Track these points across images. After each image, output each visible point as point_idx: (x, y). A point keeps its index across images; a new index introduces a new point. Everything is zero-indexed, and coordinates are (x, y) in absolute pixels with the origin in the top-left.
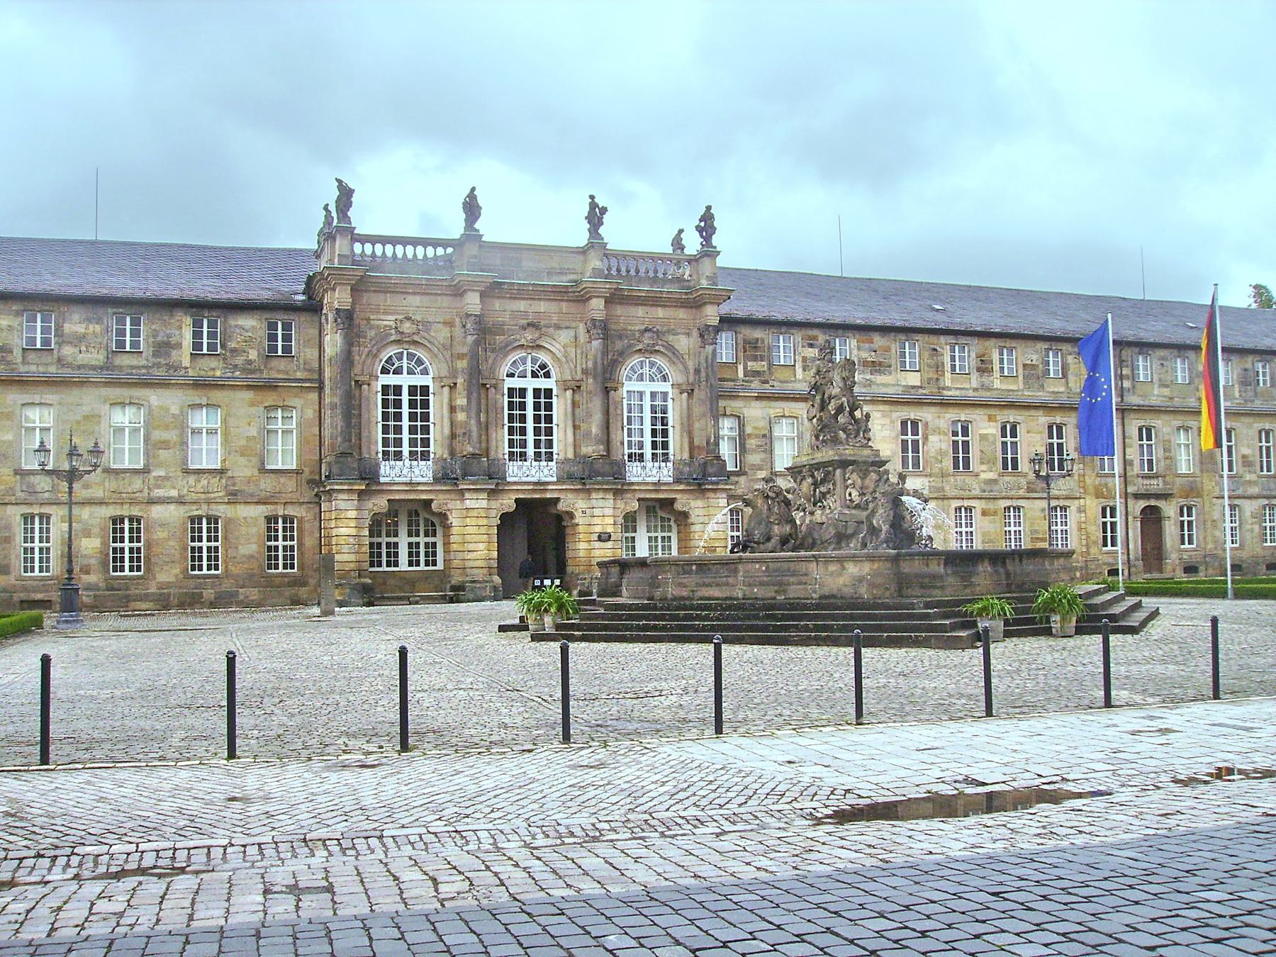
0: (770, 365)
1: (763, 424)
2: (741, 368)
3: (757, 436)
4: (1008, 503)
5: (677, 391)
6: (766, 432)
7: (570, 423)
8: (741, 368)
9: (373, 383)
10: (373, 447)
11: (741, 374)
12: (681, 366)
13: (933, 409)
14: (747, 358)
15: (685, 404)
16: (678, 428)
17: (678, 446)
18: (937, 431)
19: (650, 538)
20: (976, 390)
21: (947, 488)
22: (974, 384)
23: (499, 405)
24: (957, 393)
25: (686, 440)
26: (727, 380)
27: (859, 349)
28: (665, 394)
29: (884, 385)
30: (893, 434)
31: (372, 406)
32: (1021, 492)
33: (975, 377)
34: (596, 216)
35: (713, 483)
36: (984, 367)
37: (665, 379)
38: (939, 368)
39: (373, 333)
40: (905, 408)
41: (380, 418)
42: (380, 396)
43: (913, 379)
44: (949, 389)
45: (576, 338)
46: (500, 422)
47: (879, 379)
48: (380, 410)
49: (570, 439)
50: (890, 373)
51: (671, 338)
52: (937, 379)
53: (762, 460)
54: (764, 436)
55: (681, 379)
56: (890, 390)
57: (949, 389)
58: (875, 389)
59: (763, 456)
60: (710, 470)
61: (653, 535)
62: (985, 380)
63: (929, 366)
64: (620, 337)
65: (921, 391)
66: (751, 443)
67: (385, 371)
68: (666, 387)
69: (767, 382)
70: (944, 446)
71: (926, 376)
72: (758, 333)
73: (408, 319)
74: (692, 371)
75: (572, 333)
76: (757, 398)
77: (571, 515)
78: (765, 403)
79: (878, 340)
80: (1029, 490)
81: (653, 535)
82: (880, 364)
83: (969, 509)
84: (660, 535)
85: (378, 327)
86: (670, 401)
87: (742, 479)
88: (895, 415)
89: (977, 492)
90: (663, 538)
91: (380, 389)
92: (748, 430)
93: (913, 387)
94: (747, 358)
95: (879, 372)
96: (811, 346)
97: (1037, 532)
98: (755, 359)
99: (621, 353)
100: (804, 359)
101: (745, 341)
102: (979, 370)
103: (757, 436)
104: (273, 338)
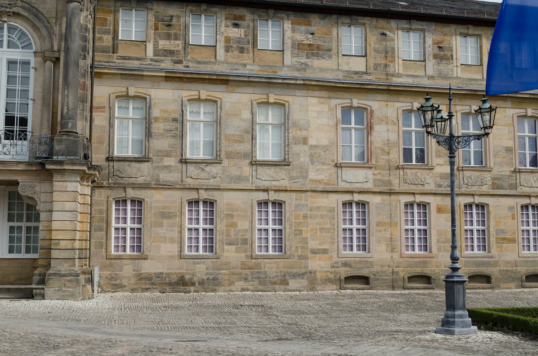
0: (186, 44)
1: (174, 107)
2: (150, 47)
3: (166, 120)
4: (469, 200)
5: (39, 59)
6: (177, 116)
8: (150, 47)
11: (150, 52)
12: (44, 32)
13: (379, 97)
16: (39, 102)
17: (38, 121)
18: (385, 120)
19: (12, 229)
20: (432, 77)
21: (396, 182)
22: (430, 71)
24: (409, 81)
25: (47, 116)
26: (130, 58)
27: (293, 31)
28: (26, 63)
29: (322, 70)
30: (332, 122)
32: (485, 189)
33: (431, 63)
35: (61, 163)
36: (443, 54)
37: (28, 46)
38: (389, 53)
40: (347, 95)
43: (359, 65)
44: (399, 75)
47: (316, 63)
50: (330, 57)
52: (386, 66)
53: (170, 146)
54: (175, 120)
56: (329, 76)
57: (399, 75)
58: (309, 74)
59: (172, 141)
60: (57, 147)
61: (15, 224)
62: (444, 67)
63: (376, 51)
65: (366, 77)
66: (158, 127)
68: (28, 55)
69: (180, 62)
70: (393, 137)
71: (372, 62)
76: (168, 79)
78: (176, 85)
79: (318, 24)
80: (495, 186)
81: (15, 224)
82: (318, 47)
83: (423, 206)
84: (24, 224)
86: (32, 71)
87: (145, 165)
88: (334, 102)
89: (431, 187)
90: (28, 229)
92: (156, 113)
93: (356, 73)
95: (317, 56)
96: (236, 25)
97: (503, 231)
98: (168, 37)
100: (228, 40)
102: (435, 56)
103: (166, 120)
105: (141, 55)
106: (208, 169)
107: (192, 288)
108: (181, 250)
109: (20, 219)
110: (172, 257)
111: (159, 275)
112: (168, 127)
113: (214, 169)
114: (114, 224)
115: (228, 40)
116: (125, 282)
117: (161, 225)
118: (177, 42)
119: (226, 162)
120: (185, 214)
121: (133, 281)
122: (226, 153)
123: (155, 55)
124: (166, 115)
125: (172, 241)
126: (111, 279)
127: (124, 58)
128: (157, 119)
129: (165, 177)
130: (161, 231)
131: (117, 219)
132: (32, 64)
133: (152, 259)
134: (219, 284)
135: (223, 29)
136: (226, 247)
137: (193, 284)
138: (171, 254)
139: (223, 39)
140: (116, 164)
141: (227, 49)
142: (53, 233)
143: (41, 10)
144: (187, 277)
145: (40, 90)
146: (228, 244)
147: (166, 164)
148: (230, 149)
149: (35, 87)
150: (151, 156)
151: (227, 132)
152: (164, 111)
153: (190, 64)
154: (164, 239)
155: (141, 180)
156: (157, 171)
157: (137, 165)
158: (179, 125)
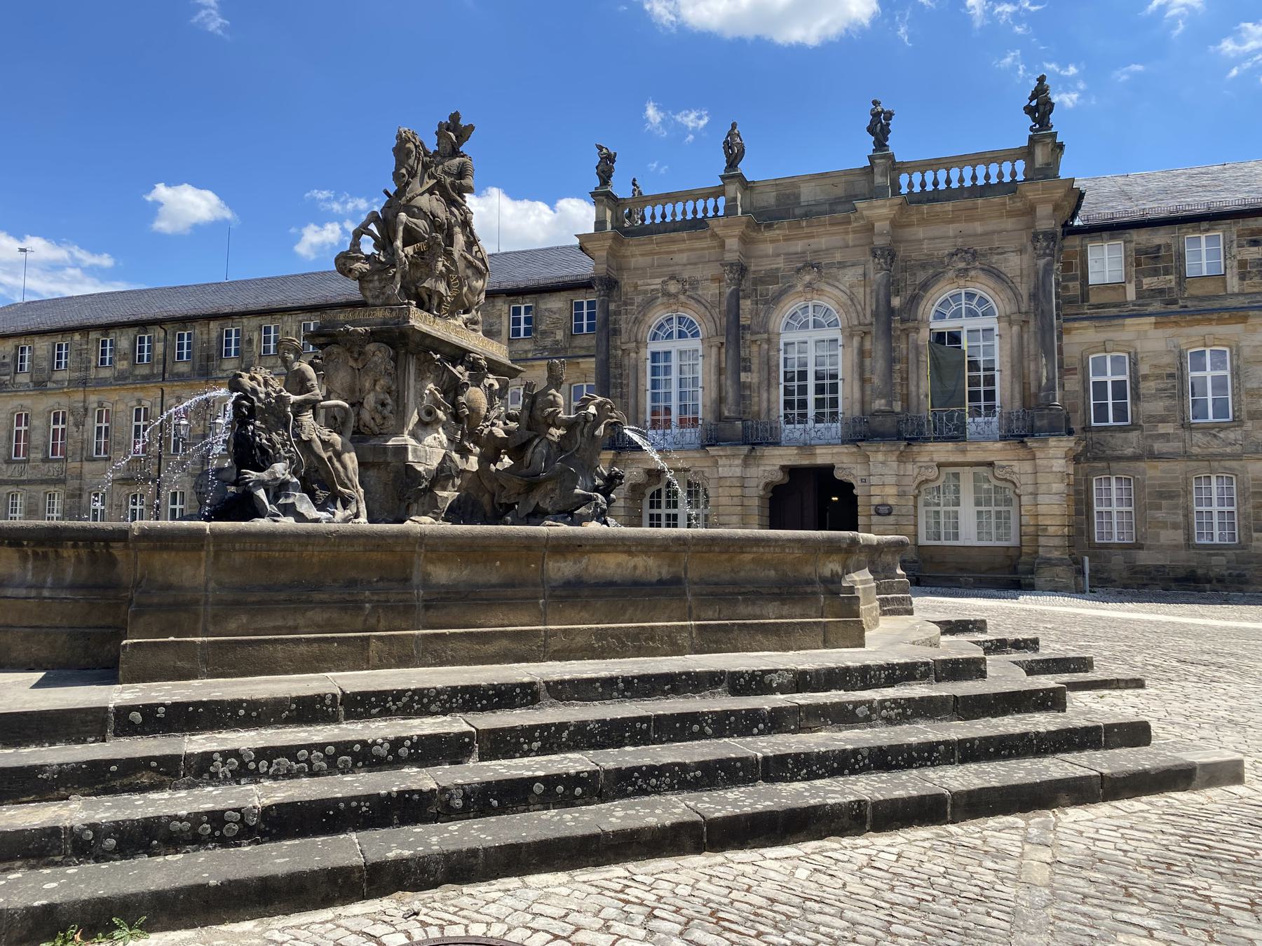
0: (1182, 278)
3: (1158, 377)
7: (856, 376)
9: (642, 351)
10: (641, 416)
14: (1141, 273)
15: (1015, 340)
16: (1007, 372)
17: (1008, 393)
19: (979, 513)
23: (773, 363)
31: (641, 375)
34: (879, 127)
39: (640, 298)
41: (649, 386)
42: (649, 363)
45: (865, 275)
46: (773, 382)
48: (649, 377)
49: (857, 395)
51: (995, 258)
53: (1167, 409)
54: (1171, 376)
55: (1009, 308)
59: (1168, 402)
64: (923, 266)
67: (655, 337)
69: (1174, 302)
72: (1159, 237)
73: (672, 278)
74: (1025, 297)
75: (860, 270)
77: (851, 486)
84: (993, 509)
85: (645, 292)
87: (1134, 436)
91: (649, 356)
92: (1144, 369)
94: (1141, 273)
98: (1155, 272)
99: (925, 286)
100: (1242, 264)
101: (1138, 252)
103: (1158, 377)
104: (579, 317)
105: (1120, 299)
106: (1222, 435)
107: (1208, 586)
108: (1189, 537)
109: (988, 503)
110: (1176, 546)
111: (1160, 568)
112: (1162, 386)
113: (1231, 435)
114: (1096, 508)
115: (1242, 264)
116: (1114, 576)
117: (1159, 508)
118: (1168, 277)
119: (1249, 425)
120: (1191, 493)
121: (1125, 574)
122: (1249, 412)
123: (1138, 297)
124: (1158, 371)
125: (1175, 526)
126: (1097, 571)
127: (1097, 306)
128: (1145, 377)
129: (1158, 446)
130: (1160, 515)
131: (1100, 501)
132: (996, 332)
133: (1149, 549)
134: (1247, 582)
135: (1235, 250)
136: (1255, 535)
137: (1209, 581)
138: (1174, 543)
139: (1235, 264)
140: (1095, 436)
141: (1242, 277)
142: (1040, 518)
143: (1003, 269)
144: (1200, 572)
145: (1007, 359)
146: (1256, 531)
147: (1162, 431)
148: (1254, 407)
149: (1001, 356)
150: (1141, 422)
151: (1248, 386)
152: (1155, 366)
153: (1189, 304)
154: (1164, 525)
155: (1129, 451)
156: (1149, 441)
157: (1123, 435)
158: (1176, 382)
